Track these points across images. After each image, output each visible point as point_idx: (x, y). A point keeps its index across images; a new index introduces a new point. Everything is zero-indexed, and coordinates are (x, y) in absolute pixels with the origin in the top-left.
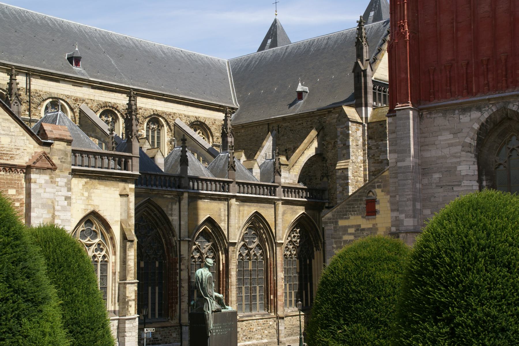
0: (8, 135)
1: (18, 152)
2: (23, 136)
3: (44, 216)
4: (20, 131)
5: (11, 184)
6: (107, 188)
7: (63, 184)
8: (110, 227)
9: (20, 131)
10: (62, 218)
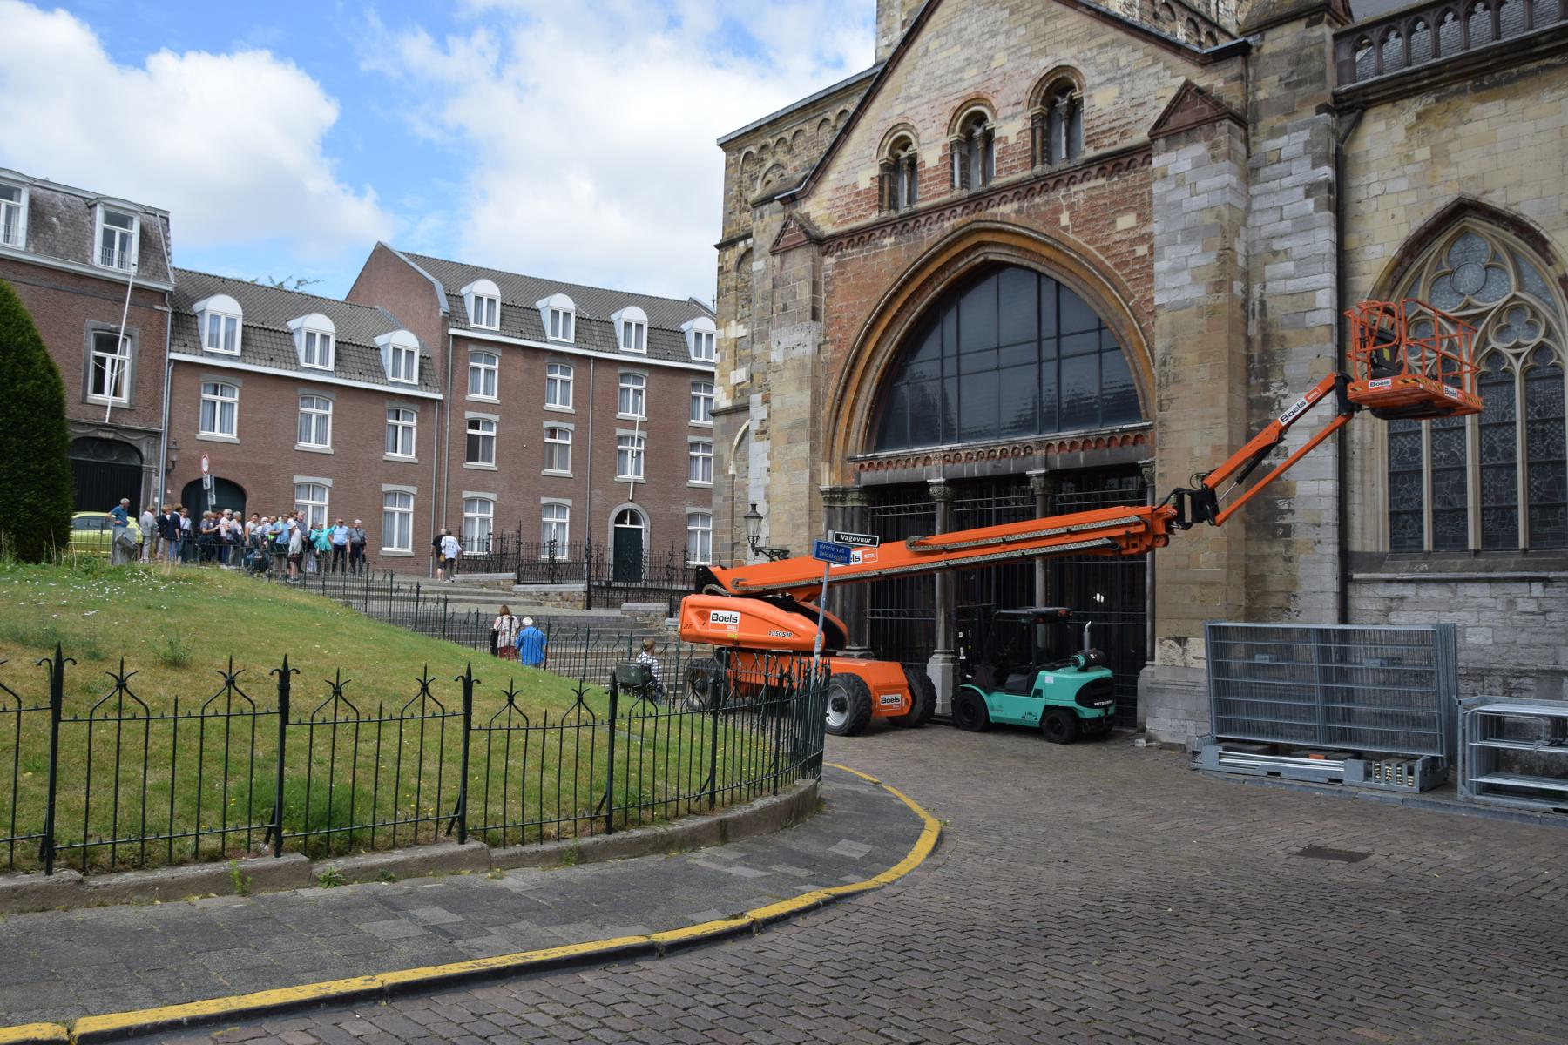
0: (1111, 80)
1: (1141, 113)
2: (1156, 61)
3: (1193, 262)
4: (1146, 55)
5: (1124, 201)
6: (1515, 105)
7: (1298, 148)
8: (1544, 242)
9: (1146, 55)
10: (1295, 254)
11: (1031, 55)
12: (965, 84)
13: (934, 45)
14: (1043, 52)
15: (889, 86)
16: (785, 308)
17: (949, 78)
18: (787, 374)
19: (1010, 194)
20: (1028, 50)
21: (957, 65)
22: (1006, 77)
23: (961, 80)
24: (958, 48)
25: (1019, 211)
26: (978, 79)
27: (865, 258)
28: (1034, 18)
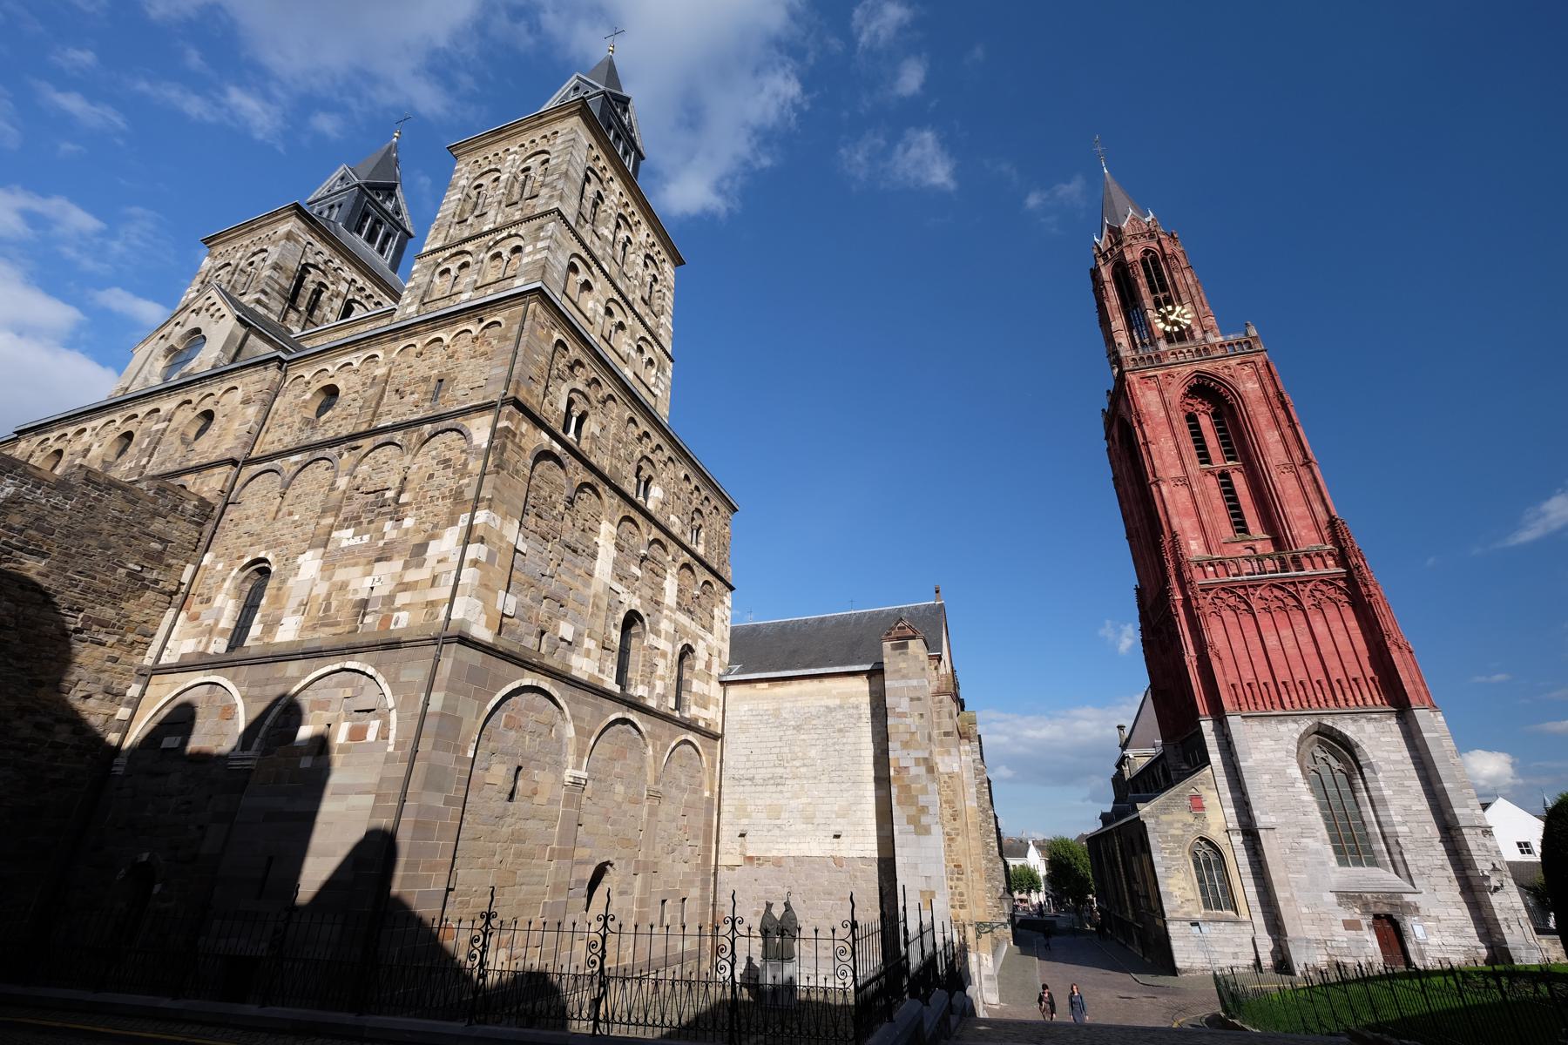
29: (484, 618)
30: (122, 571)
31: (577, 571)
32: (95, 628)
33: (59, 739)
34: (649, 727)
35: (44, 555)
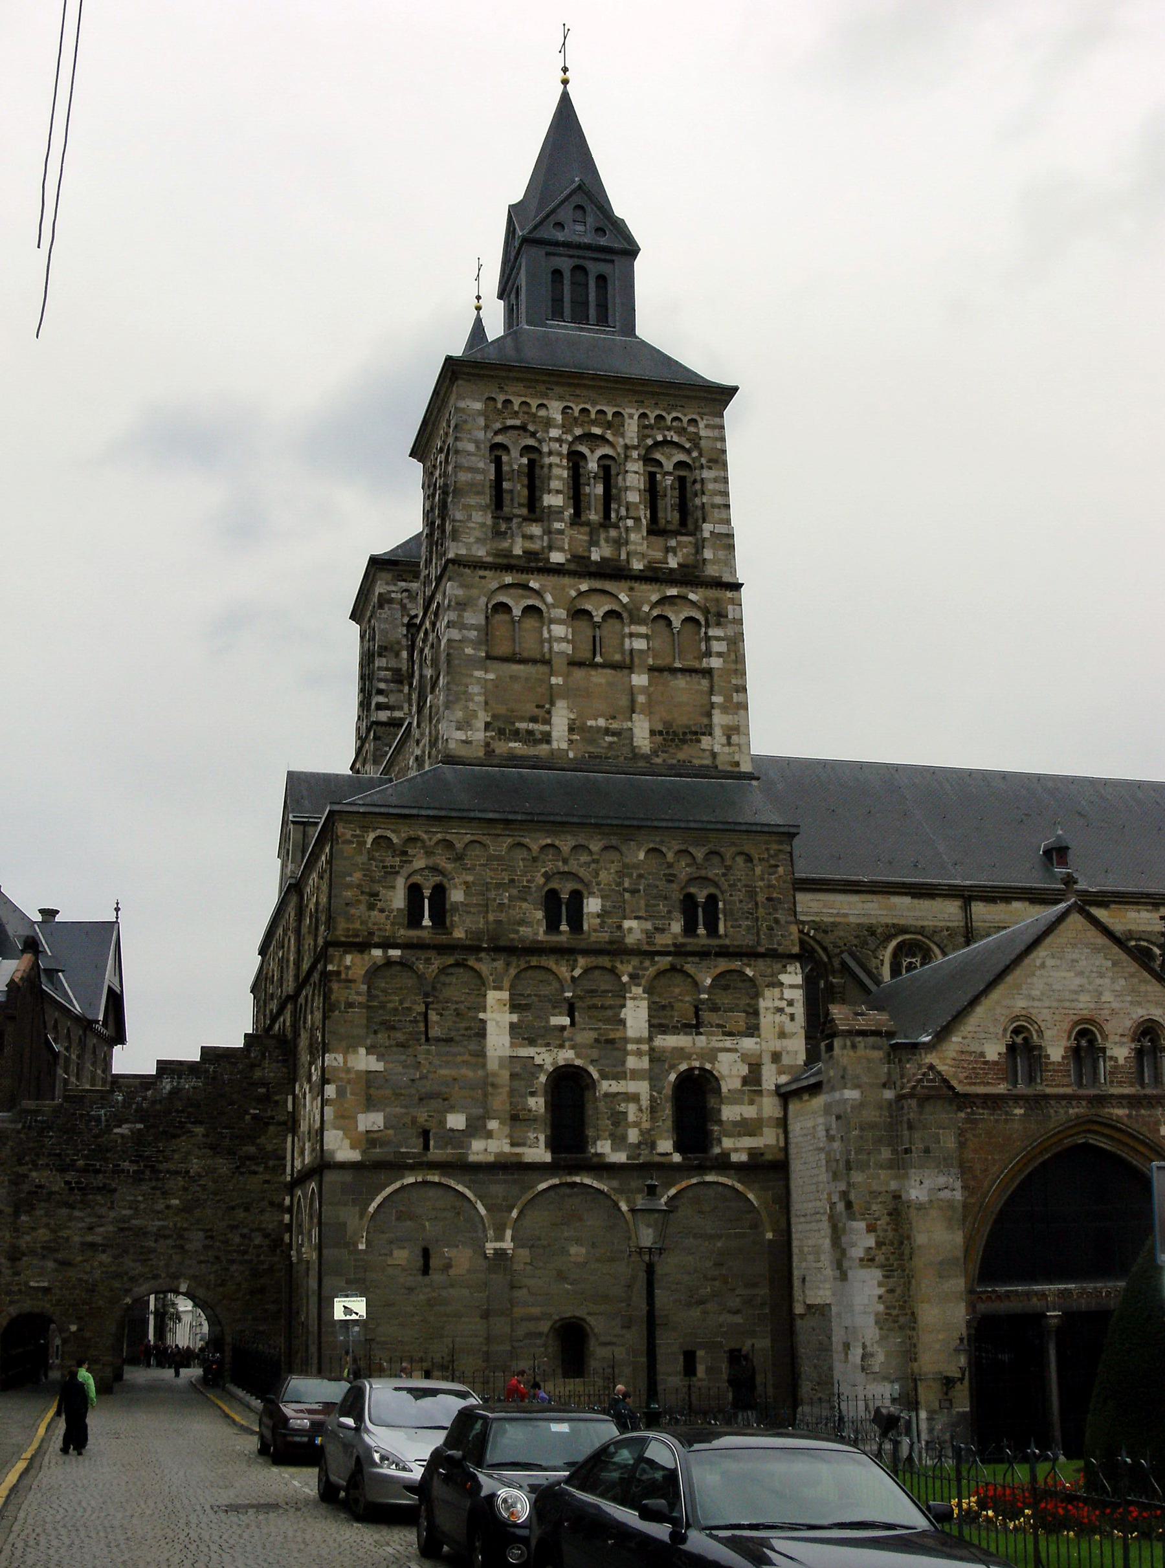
11: (1131, 1003)
12: (1081, 1006)
13: (1050, 962)
14: (1139, 1004)
15: (1010, 979)
16: (927, 1150)
17: (1067, 996)
18: (934, 1213)
19: (1124, 1102)
20: (1129, 998)
21: (1072, 988)
22: (1113, 1012)
23: (1077, 1000)
24: (1072, 974)
25: (1129, 1116)
26: (1092, 1006)
27: (997, 1121)
28: (1132, 976)
29: (347, 1142)
30: (248, 1117)
31: (459, 1059)
32: (248, 1163)
33: (257, 1242)
34: (615, 1184)
35: (201, 1123)
